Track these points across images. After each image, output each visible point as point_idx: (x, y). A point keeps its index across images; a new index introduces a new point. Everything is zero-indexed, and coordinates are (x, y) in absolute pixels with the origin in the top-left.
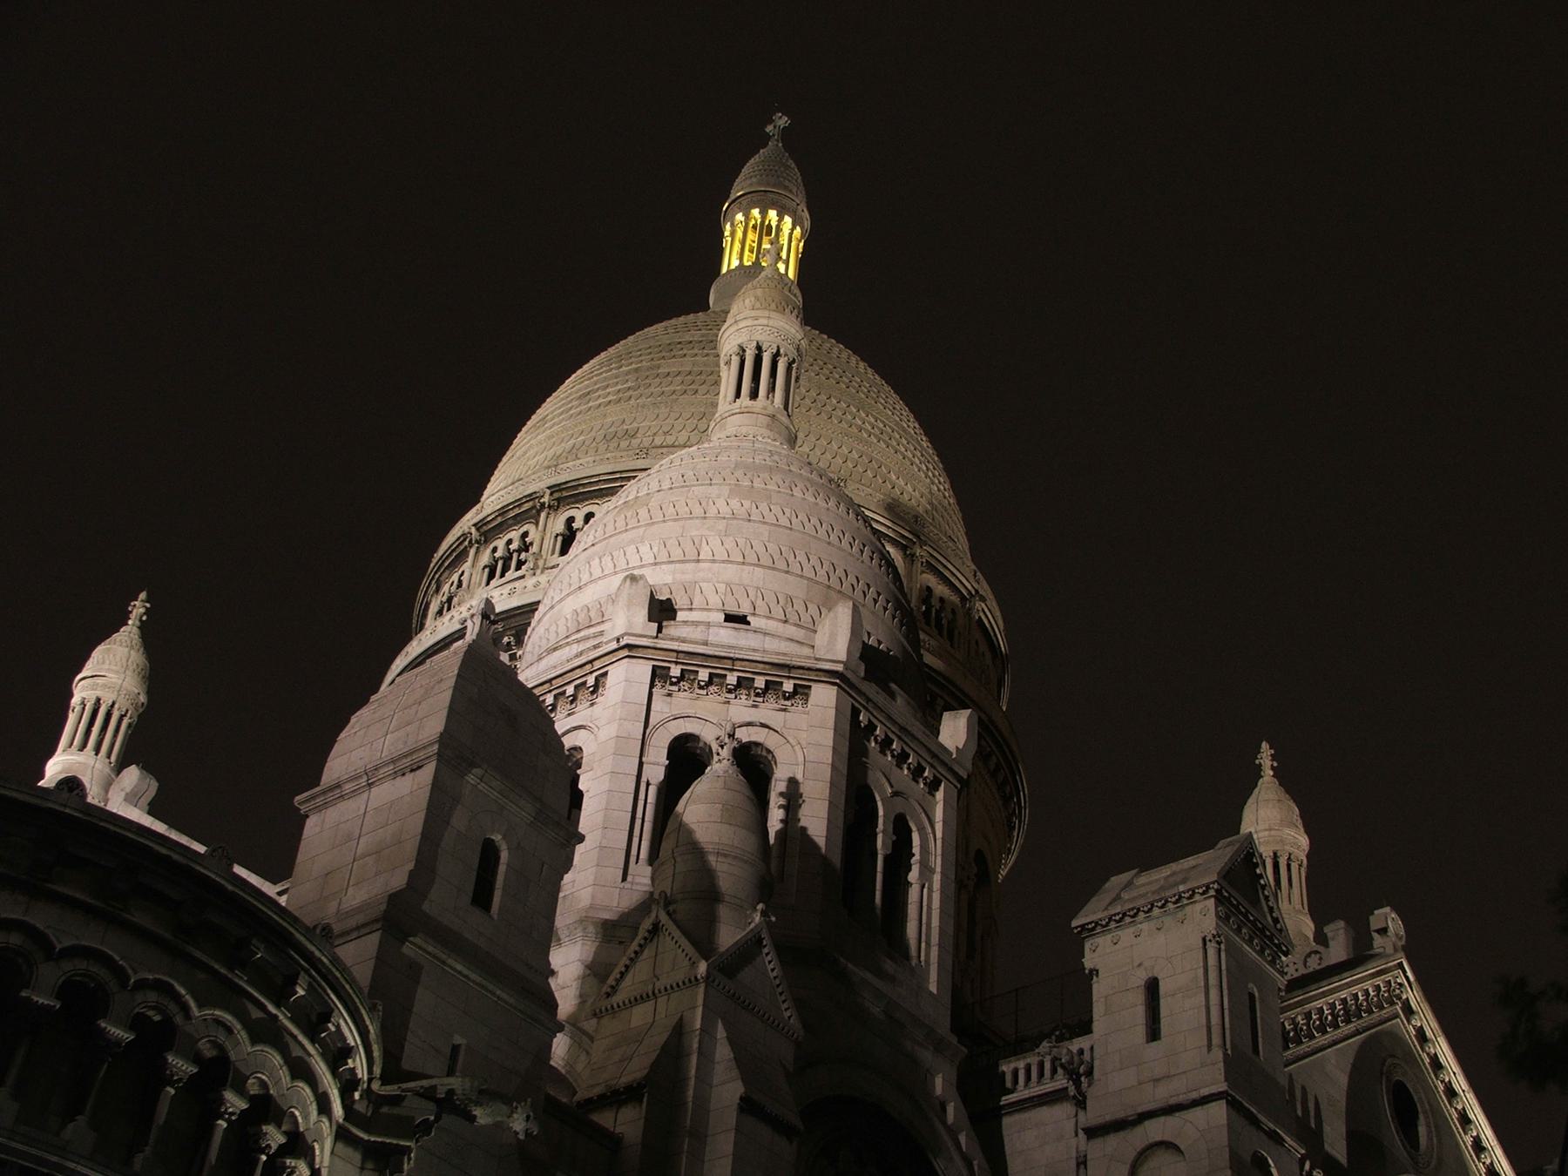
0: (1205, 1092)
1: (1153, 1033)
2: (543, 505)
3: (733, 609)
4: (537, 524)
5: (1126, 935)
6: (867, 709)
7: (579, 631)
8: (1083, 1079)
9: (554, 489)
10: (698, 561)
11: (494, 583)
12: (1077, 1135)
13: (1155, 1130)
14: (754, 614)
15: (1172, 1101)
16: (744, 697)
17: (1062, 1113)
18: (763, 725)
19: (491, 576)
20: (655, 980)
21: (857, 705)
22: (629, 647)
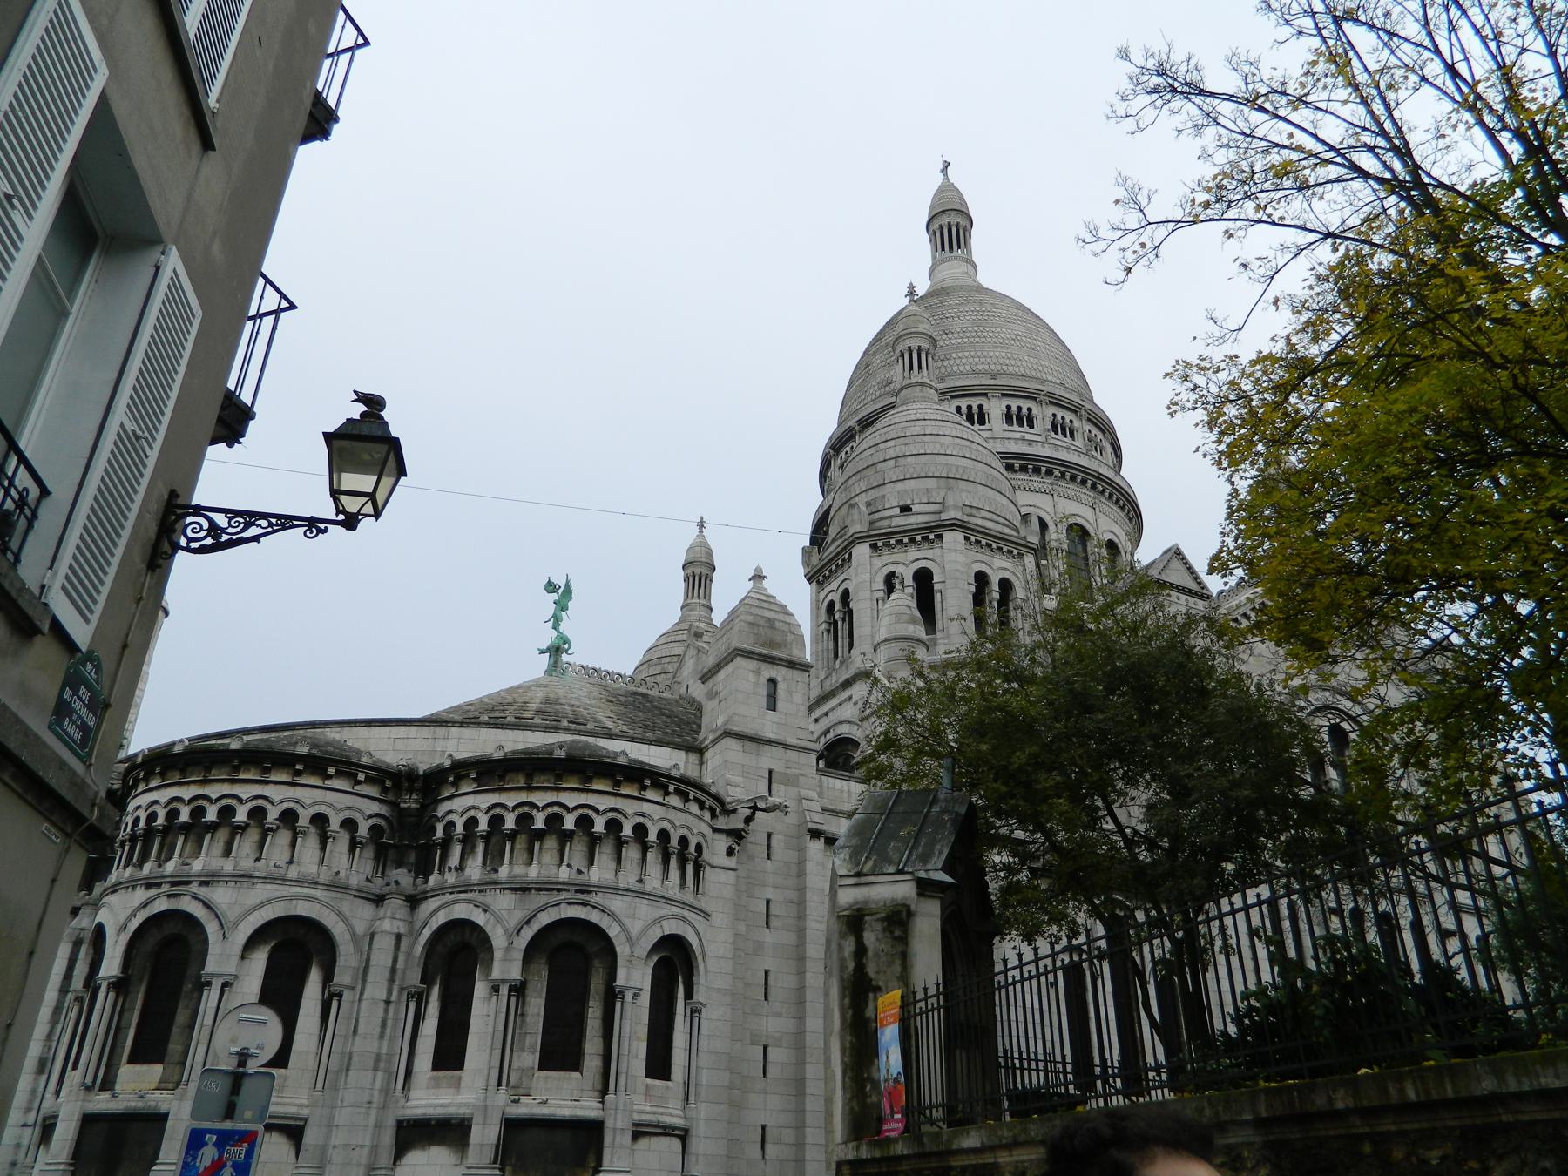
3: (902, 503)
9: (860, 422)
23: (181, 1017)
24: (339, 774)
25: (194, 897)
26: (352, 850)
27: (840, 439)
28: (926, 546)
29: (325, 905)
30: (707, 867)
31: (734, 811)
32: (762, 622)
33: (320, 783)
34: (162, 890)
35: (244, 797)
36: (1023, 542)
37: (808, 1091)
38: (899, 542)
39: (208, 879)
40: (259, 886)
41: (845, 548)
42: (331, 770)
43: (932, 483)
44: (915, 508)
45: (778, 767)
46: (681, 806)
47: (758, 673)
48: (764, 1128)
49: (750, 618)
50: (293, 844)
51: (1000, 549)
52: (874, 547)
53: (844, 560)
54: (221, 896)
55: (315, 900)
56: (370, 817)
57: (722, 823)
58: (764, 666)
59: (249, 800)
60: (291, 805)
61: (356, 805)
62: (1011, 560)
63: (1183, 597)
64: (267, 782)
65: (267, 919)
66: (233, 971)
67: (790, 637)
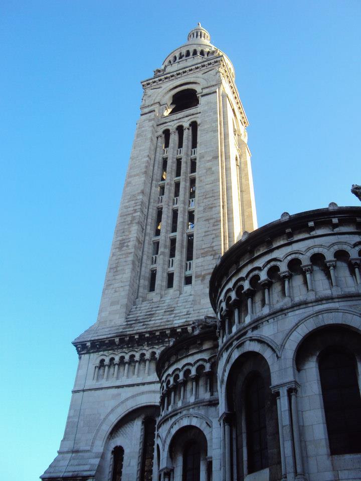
23: (270, 429)
24: (318, 226)
25: (251, 340)
26: (353, 273)
29: (345, 312)
33: (307, 236)
34: (234, 346)
35: (261, 265)
39: (256, 324)
40: (290, 314)
42: (311, 224)
50: (305, 282)
54: (267, 331)
55: (336, 310)
56: (355, 245)
59: (264, 266)
60: (293, 256)
61: (340, 241)
64: (272, 251)
65: (304, 334)
66: (291, 378)
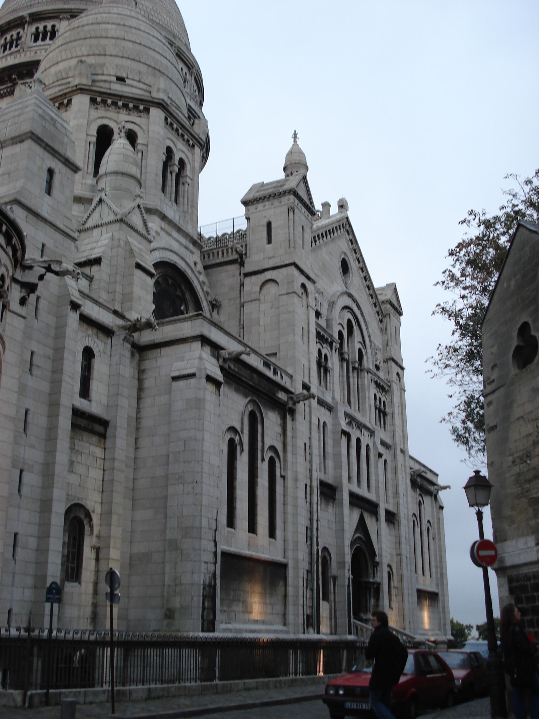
0: (287, 262)
1: (269, 241)
2: (26, 22)
3: (119, 74)
4: (24, 29)
5: (260, 206)
6: (170, 118)
7: (58, 81)
8: (243, 256)
9: (31, 15)
10: (105, 55)
11: (7, 52)
12: (240, 275)
13: (268, 275)
14: (127, 78)
15: (275, 265)
16: (125, 111)
17: (233, 269)
18: (132, 122)
19: (5, 50)
20: (101, 220)
21: (167, 116)
22: (81, 89)
27: (9, 23)
28: (135, 113)
30: (7, 310)
31: (30, 268)
32: (48, 118)
36: (197, 137)
37: (54, 509)
38: (115, 104)
41: (65, 94)
43: (143, 68)
44: (128, 81)
45: (49, 244)
46: (5, 247)
47: (43, 160)
48: (16, 535)
49: (40, 111)
51: (183, 136)
52: (93, 101)
53: (61, 104)
57: (19, 275)
58: (47, 155)
62: (187, 146)
63: (303, 209)
67: (66, 140)
